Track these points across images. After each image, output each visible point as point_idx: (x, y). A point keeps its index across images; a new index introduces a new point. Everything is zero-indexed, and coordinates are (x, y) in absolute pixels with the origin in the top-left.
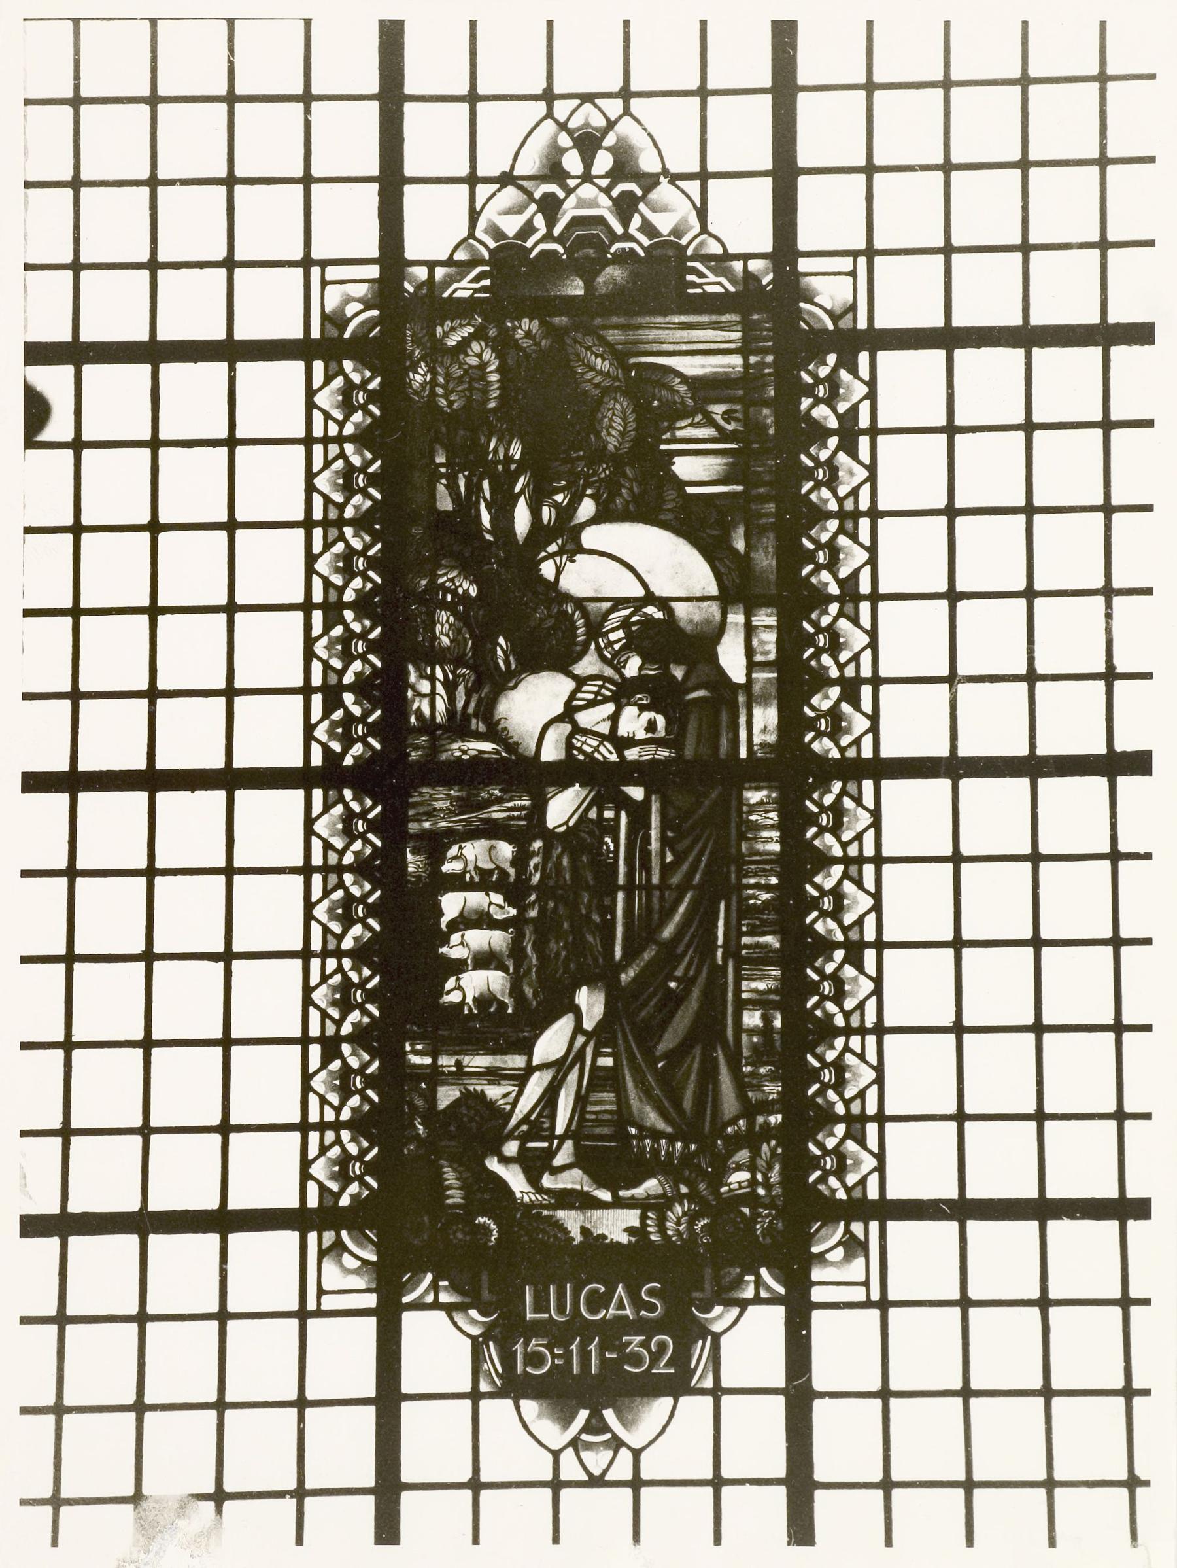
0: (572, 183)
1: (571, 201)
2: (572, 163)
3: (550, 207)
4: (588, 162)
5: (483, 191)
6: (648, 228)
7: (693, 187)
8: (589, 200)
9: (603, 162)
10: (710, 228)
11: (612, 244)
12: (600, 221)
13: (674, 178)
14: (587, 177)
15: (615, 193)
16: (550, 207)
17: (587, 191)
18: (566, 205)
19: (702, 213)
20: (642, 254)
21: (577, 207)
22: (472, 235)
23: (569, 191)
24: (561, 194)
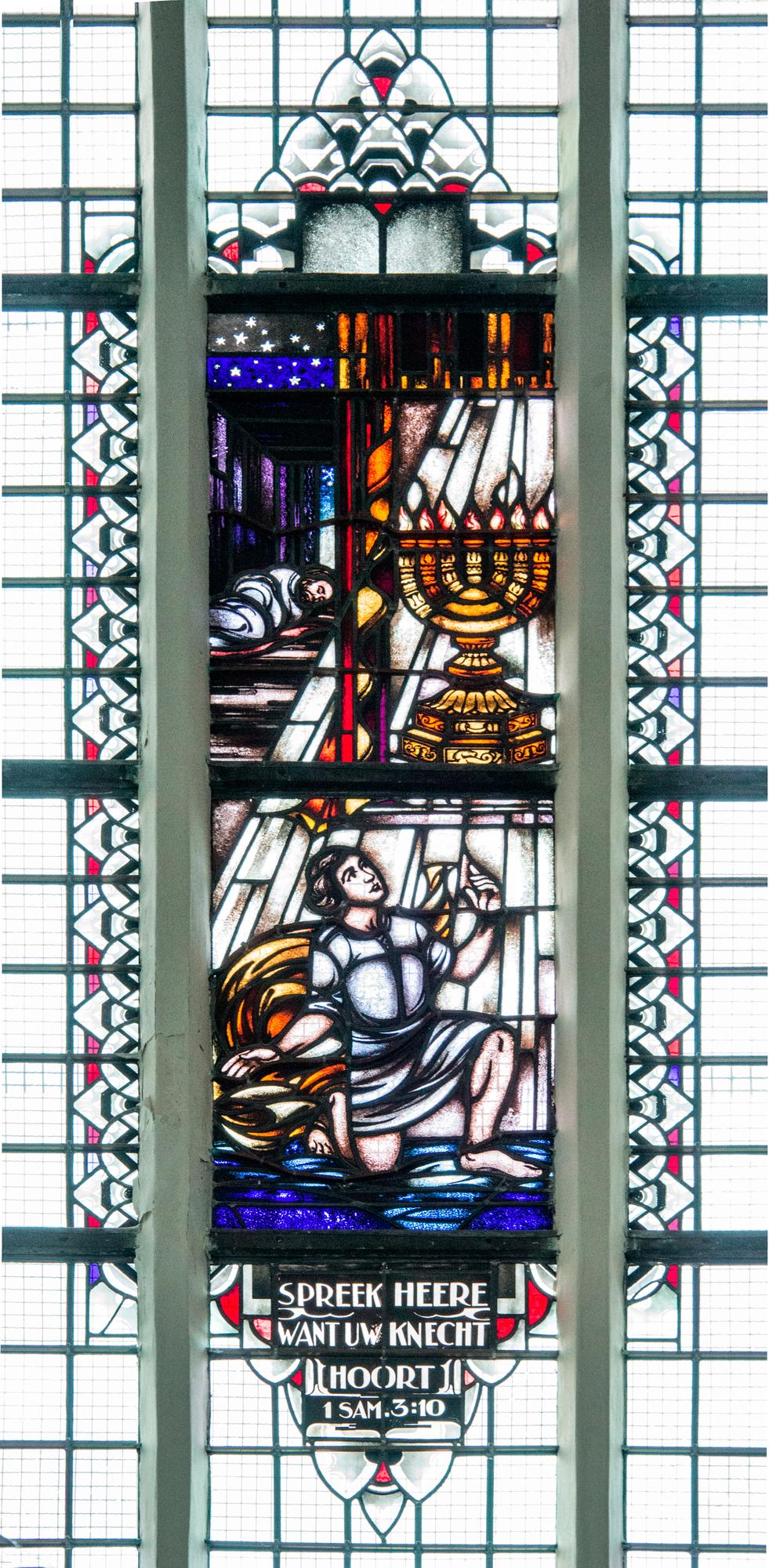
0: (369, 115)
1: (368, 134)
2: (370, 97)
3: (347, 140)
4: (383, 94)
5: (286, 122)
6: (440, 166)
7: (480, 123)
8: (381, 133)
9: (396, 98)
10: (496, 165)
11: (407, 176)
12: (394, 154)
13: (463, 113)
14: (383, 108)
15: (408, 130)
16: (347, 140)
17: (382, 124)
18: (362, 138)
19: (488, 150)
20: (432, 189)
21: (371, 140)
22: (276, 168)
23: (366, 124)
24: (358, 128)
